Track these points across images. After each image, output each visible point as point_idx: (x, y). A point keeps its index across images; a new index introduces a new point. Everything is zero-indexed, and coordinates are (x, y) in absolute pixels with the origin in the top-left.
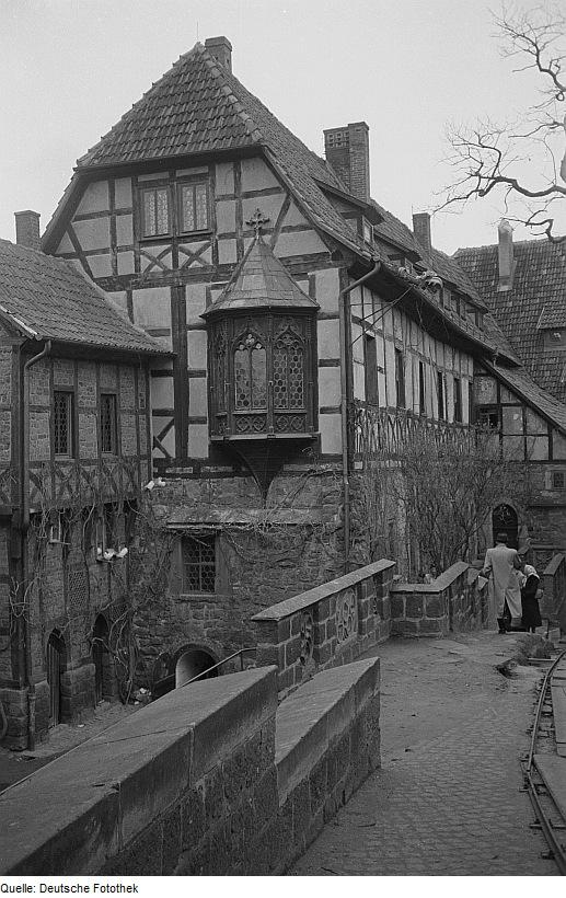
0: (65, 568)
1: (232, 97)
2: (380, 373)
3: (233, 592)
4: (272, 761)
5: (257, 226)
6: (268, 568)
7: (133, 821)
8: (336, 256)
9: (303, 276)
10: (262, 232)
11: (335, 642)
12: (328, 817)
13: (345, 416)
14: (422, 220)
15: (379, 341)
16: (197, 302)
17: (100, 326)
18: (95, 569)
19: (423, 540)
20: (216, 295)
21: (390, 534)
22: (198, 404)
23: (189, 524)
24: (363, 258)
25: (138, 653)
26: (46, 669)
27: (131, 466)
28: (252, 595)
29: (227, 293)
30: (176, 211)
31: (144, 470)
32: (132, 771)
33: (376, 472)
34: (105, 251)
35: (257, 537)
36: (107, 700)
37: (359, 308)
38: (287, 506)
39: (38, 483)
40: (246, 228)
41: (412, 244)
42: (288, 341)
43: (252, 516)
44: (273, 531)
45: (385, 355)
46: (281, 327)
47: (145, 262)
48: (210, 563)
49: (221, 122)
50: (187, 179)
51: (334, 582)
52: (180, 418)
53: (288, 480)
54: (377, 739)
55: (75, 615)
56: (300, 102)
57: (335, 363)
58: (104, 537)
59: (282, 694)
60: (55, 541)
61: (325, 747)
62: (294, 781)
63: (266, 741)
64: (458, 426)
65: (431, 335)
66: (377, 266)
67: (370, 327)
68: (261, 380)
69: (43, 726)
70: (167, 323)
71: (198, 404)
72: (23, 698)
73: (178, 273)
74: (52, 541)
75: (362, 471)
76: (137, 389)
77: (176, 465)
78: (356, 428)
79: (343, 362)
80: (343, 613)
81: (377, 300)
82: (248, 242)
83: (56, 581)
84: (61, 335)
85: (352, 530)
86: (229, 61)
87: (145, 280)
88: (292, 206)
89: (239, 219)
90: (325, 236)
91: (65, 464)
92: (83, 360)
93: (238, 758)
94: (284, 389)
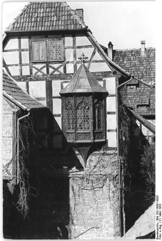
8: (114, 73)
9: (101, 80)
10: (84, 62)
16: (57, 88)
20: (65, 85)
24: (126, 75)
40: (78, 60)
47: (34, 71)
73: (49, 76)
82: (79, 66)
87: (35, 78)
89: (75, 56)
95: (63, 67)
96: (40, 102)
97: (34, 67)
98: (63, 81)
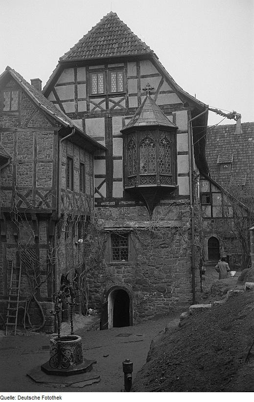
9: (170, 114)
10: (150, 94)
20: (127, 122)
23: (116, 228)
28: (147, 261)
30: (107, 83)
34: (72, 101)
35: (151, 233)
40: (142, 91)
43: (146, 224)
44: (157, 230)
46: (162, 135)
47: (92, 106)
48: (125, 247)
50: (113, 69)
52: (109, 179)
53: (163, 207)
77: (106, 200)
82: (143, 98)
87: (92, 114)
88: (165, 83)
89: (139, 88)
94: (163, 164)
95: (125, 100)
97: (91, 102)
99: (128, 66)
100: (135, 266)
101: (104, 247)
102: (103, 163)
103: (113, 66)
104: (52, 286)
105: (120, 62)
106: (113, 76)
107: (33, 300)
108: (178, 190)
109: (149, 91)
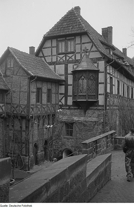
0: (38, 129)
1: (80, 20)
2: (112, 85)
3: (77, 136)
4: (86, 176)
5: (85, 51)
6: (85, 131)
7: (53, 188)
9: (96, 63)
10: (86, 52)
11: (101, 149)
12: (98, 190)
13: (105, 96)
14: (125, 50)
15: (114, 78)
17: (48, 73)
18: (45, 130)
19: (123, 126)
20: (75, 67)
21: (115, 124)
22: (70, 92)
23: (68, 120)
24: (110, 59)
25: (54, 150)
26: (33, 152)
27: (54, 106)
29: (78, 66)
30: (66, 47)
31: (57, 107)
32: (53, 177)
33: (112, 110)
34: (50, 56)
36: (47, 160)
37: (109, 70)
38: (91, 117)
39: (33, 109)
40: (83, 51)
41: (122, 55)
42: (92, 78)
43: (82, 119)
45: (115, 82)
47: (59, 59)
49: (77, 26)
50: (69, 39)
51: (101, 135)
52: (66, 95)
53: (91, 111)
54: (110, 172)
55: (40, 140)
56: (96, 22)
57: (103, 83)
58: (47, 122)
59: (88, 161)
60: (36, 123)
61: (98, 174)
62: (91, 181)
63: (84, 172)
64: (132, 99)
65: (126, 77)
66: (114, 61)
67: (112, 75)
68: (85, 87)
69: (32, 166)
70: (63, 73)
71: (70, 92)
72: (28, 159)
74: (35, 123)
75: (108, 109)
76: (56, 88)
78: (107, 99)
79: (105, 83)
80: (103, 143)
81: (113, 69)
82: (83, 54)
83: (36, 132)
84: (39, 75)
85: (106, 123)
86: (80, 12)
87: (59, 63)
88: (94, 46)
89: (81, 49)
90: (101, 53)
91: (39, 105)
92: (44, 81)
93: (78, 175)
95: (74, 56)
96: (61, 77)
97: (58, 57)
98: (74, 64)
99: (76, 38)
100: (75, 139)
101: (62, 129)
102: (63, 87)
103: (69, 38)
104: (27, 149)
105: (72, 36)
106: (69, 43)
107: (19, 155)
108: (99, 102)
109: (86, 51)
